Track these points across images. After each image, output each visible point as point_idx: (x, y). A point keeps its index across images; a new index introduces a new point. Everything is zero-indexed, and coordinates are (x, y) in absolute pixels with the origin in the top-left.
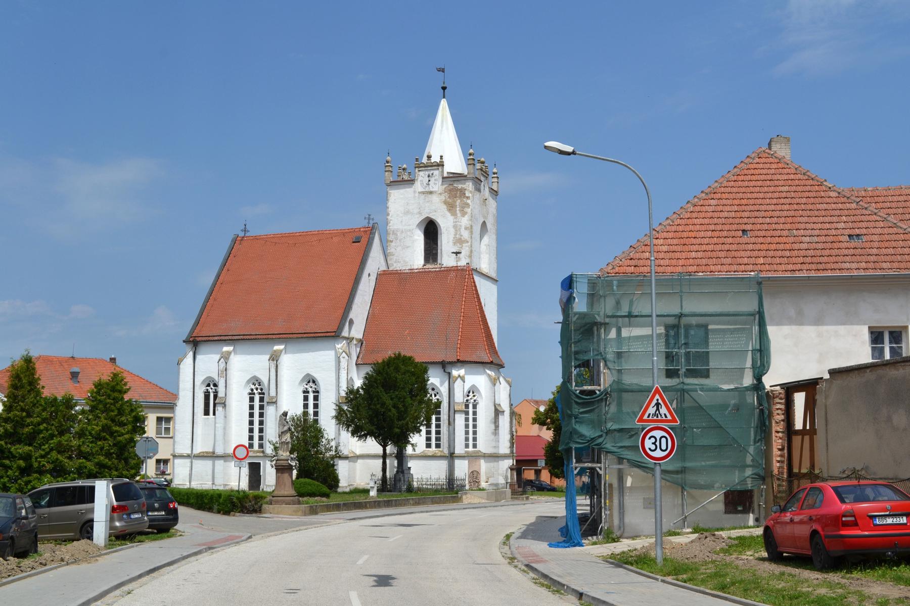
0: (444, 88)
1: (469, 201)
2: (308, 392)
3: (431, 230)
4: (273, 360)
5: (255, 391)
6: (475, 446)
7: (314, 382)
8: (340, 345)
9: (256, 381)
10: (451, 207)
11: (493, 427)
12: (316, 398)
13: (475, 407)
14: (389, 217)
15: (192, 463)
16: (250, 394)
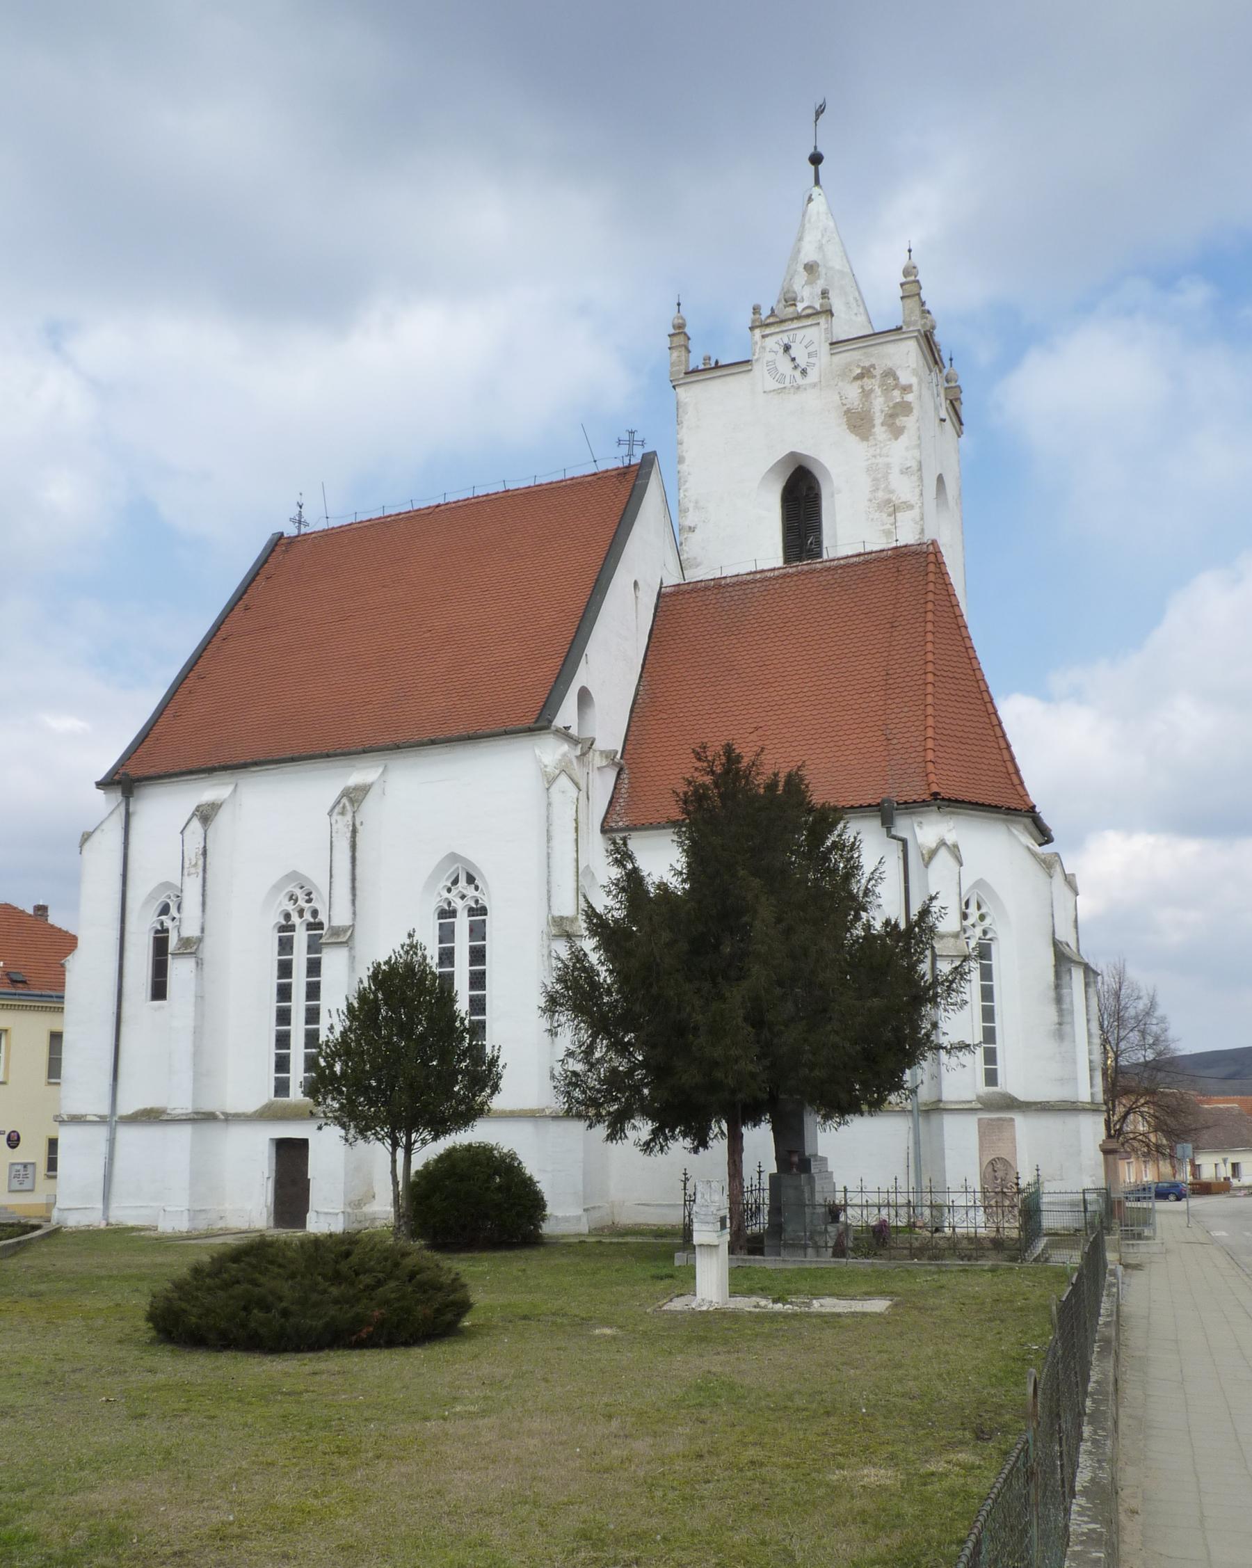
0: (816, 159)
1: (909, 398)
2: (453, 913)
3: (801, 494)
4: (343, 813)
5: (295, 919)
6: (991, 1078)
7: (471, 879)
8: (549, 751)
9: (301, 890)
10: (859, 422)
11: (1051, 1013)
12: (478, 931)
14: (684, 468)
15: (112, 1142)
16: (282, 929)
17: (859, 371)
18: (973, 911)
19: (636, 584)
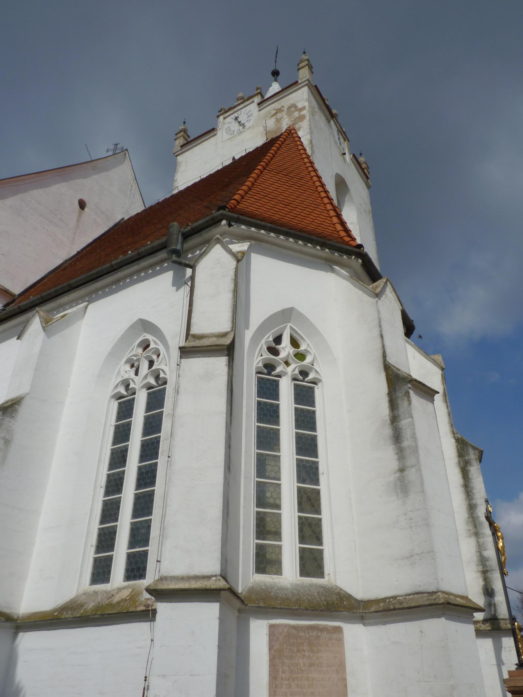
1: (304, 112)
6: (312, 563)
11: (388, 456)
13: (305, 395)
17: (275, 112)
18: (286, 349)
19: (82, 205)
